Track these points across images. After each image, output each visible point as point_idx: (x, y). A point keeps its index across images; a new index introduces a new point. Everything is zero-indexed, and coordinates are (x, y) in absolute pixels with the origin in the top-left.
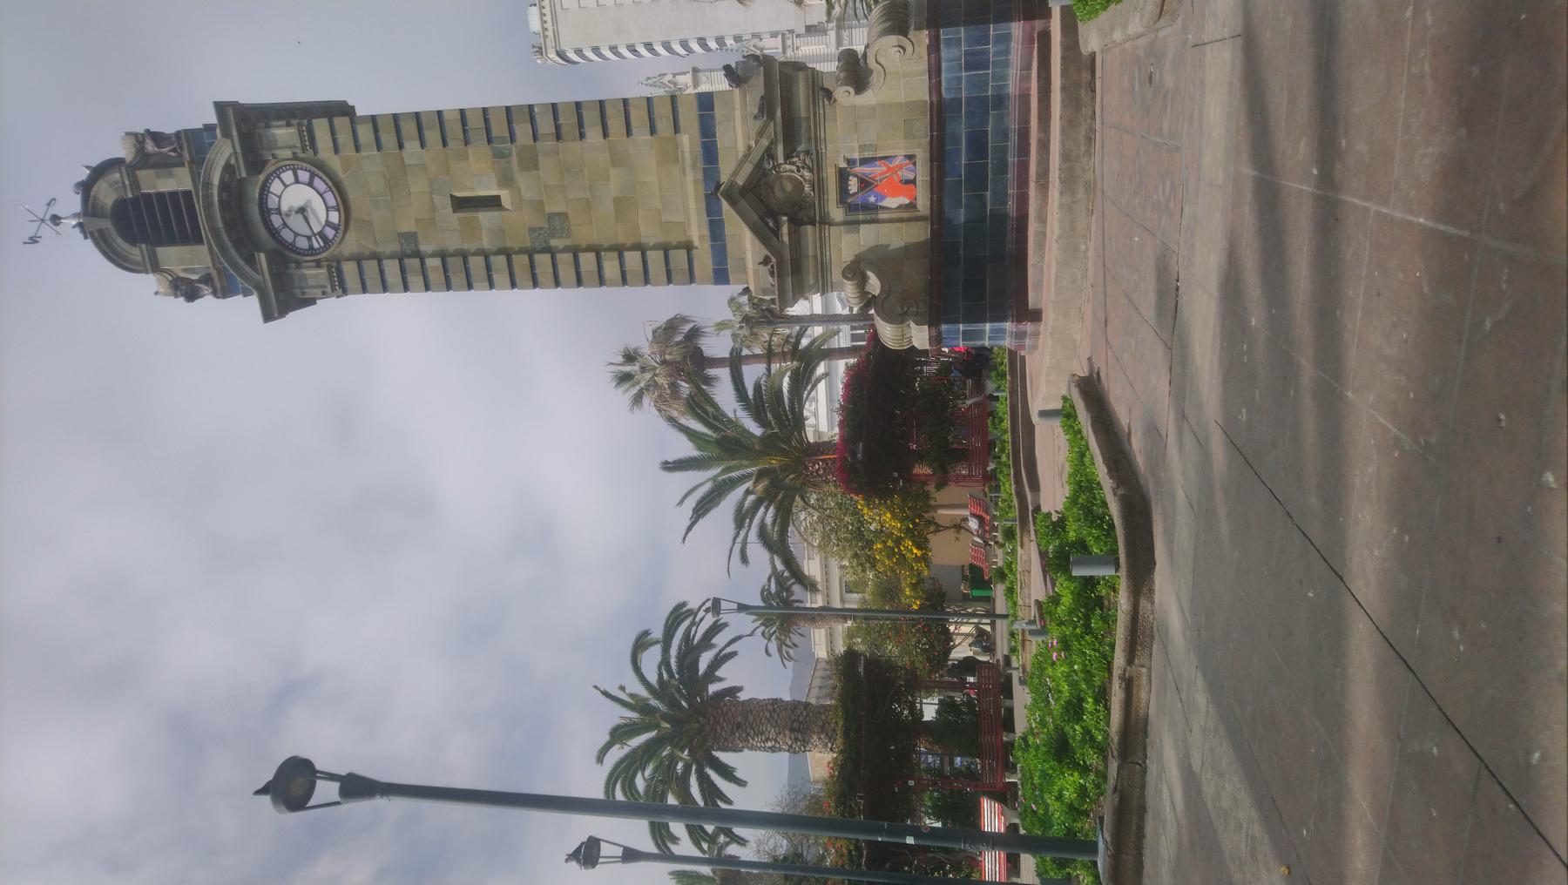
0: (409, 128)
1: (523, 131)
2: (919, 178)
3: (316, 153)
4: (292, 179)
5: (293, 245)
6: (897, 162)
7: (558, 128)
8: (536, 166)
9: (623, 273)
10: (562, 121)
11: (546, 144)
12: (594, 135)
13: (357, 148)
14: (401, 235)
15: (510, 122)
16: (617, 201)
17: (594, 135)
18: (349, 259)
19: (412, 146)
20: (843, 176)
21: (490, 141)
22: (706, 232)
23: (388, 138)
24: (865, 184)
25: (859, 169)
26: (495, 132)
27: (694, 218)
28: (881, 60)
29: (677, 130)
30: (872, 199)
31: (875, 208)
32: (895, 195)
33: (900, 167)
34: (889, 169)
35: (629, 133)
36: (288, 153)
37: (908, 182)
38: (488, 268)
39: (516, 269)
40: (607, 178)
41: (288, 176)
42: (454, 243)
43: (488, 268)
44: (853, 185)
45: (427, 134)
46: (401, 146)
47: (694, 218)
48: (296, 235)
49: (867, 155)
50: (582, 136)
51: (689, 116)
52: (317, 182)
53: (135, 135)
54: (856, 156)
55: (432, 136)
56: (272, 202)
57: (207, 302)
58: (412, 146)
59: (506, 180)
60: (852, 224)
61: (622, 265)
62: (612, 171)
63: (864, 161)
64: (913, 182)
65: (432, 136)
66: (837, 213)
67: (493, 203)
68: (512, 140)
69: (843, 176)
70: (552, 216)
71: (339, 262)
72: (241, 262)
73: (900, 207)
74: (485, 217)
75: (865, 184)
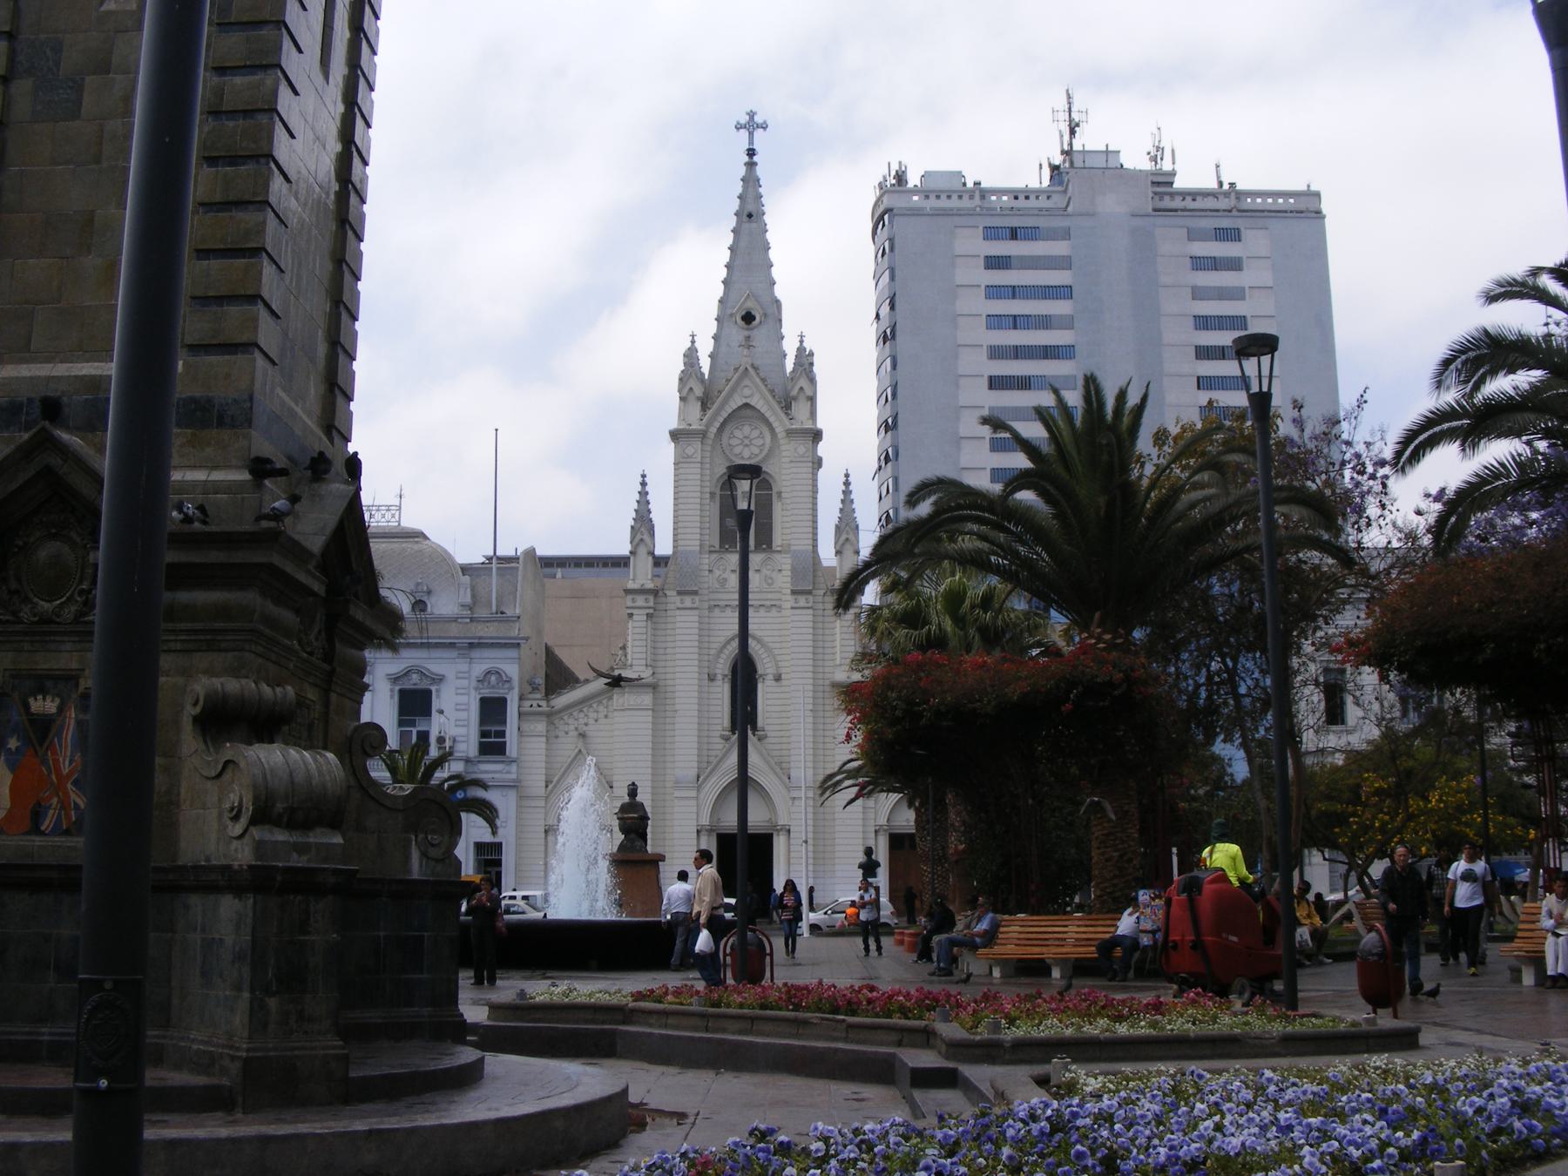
2: (38, 841)
7: (233, 114)
28: (231, 766)
33: (64, 805)
37: (37, 815)
44: (44, 705)
64: (36, 830)
75: (43, 728)
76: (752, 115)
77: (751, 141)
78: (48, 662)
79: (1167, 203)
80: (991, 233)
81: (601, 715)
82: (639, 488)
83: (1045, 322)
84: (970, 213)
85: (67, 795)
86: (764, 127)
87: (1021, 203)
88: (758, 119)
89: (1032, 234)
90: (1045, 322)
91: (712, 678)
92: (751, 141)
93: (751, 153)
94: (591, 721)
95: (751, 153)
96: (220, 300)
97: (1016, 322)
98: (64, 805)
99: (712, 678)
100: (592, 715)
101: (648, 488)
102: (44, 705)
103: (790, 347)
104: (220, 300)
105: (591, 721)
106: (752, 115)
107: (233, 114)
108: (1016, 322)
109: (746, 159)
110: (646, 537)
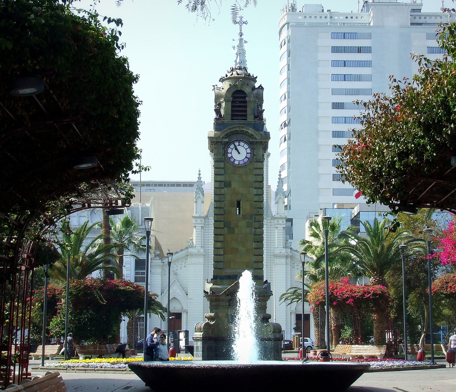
0: (259, 191)
1: (257, 225)
7: (257, 235)
9: (217, 248)
11: (254, 230)
12: (254, 245)
13: (255, 175)
16: (237, 249)
17: (254, 245)
18: (225, 165)
21: (255, 215)
22: (228, 275)
23: (257, 185)
35: (255, 255)
38: (221, 208)
41: (249, 151)
42: (228, 198)
43: (221, 208)
46: (255, 188)
50: (255, 242)
52: (247, 160)
55: (256, 198)
56: (242, 144)
57: (214, 115)
58: (255, 191)
61: (220, 248)
65: (256, 198)
68: (255, 222)
70: (234, 229)
71: (224, 162)
72: (226, 133)
77: (241, 30)
79: (417, 20)
80: (335, 36)
81: (183, 266)
82: (198, 176)
83: (359, 78)
84: (325, 25)
86: (245, 23)
87: (349, 20)
88: (244, 20)
89: (354, 36)
90: (359, 78)
92: (241, 30)
94: (179, 269)
96: (258, 262)
97: (345, 78)
100: (179, 266)
101: (201, 176)
104: (258, 262)
105: (179, 269)
107: (257, 235)
108: (345, 78)
110: (201, 196)
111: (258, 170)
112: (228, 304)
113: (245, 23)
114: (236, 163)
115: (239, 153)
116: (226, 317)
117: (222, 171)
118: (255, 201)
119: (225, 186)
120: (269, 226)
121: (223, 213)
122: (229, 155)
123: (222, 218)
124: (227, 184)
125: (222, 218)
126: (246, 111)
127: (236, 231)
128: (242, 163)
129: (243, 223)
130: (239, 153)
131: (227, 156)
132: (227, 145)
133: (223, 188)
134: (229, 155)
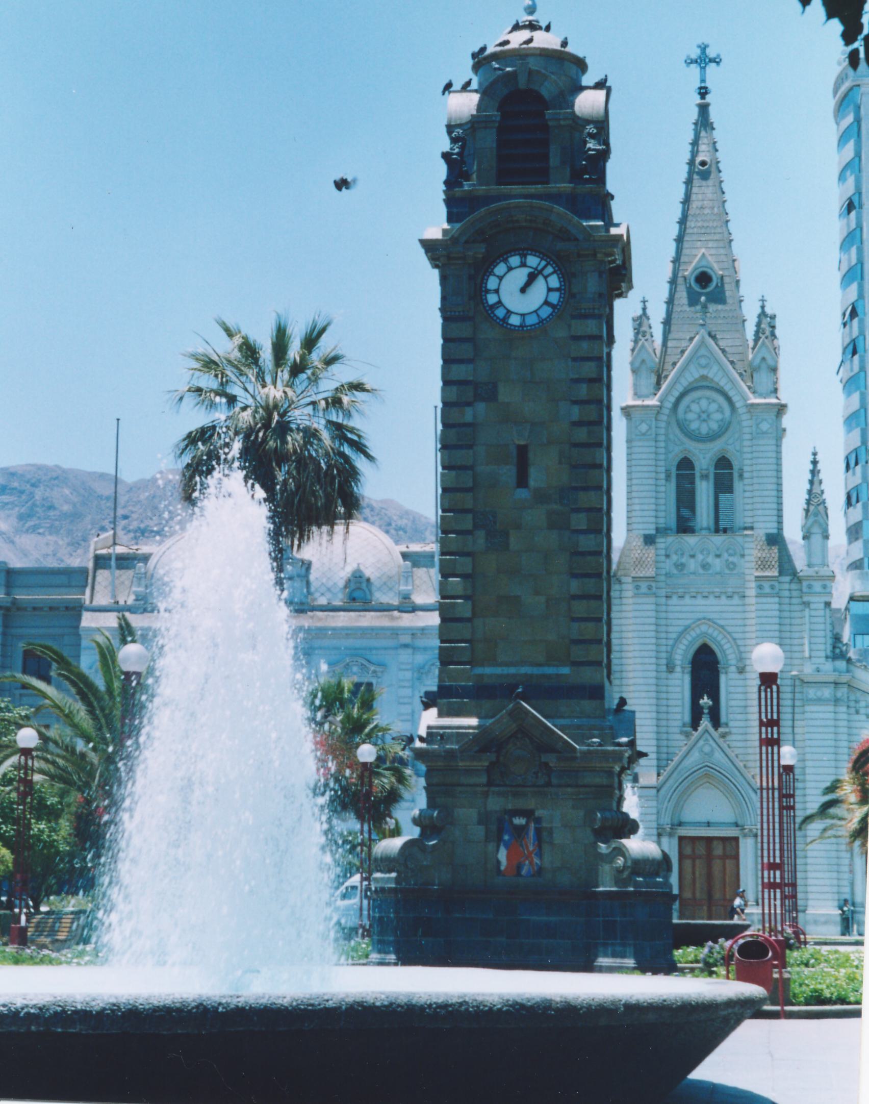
3: (573, 317)
4: (550, 300)
5: (491, 273)
6: (536, 861)
7: (583, 554)
8: (551, 526)
10: (589, 558)
14: (495, 386)
15: (590, 510)
19: (576, 412)
20: (528, 814)
23: (583, 391)
24: (520, 831)
25: (532, 825)
26: (582, 495)
27: (498, 670)
29: (575, 664)
30: (506, 837)
31: (499, 840)
32: (509, 857)
33: (531, 863)
34: (530, 853)
36: (575, 290)
39: (459, 495)
40: (537, 593)
44: (519, 821)
45: (584, 430)
47: (498, 670)
48: (501, 278)
49: (545, 834)
50: (575, 576)
51: (587, 675)
52: (546, 312)
53: (606, 80)
54: (544, 825)
55: (582, 434)
58: (576, 412)
59: (541, 497)
60: (483, 819)
62: (543, 599)
63: (538, 831)
64: (518, 874)
65: (582, 434)
66: (495, 804)
67: (522, 481)
69: (528, 814)
73: (499, 862)
74: (508, 473)
75: (520, 831)
76: (703, 48)
78: (521, 804)
85: (532, 860)
86: (716, 61)
88: (711, 53)
91: (670, 668)
92: (703, 81)
93: (703, 92)
95: (703, 92)
98: (531, 863)
99: (670, 668)
102: (519, 821)
103: (750, 313)
106: (703, 48)
109: (698, 100)
111: (585, 345)
112: (484, 779)
113: (716, 61)
114: (515, 320)
115: (523, 290)
116: (480, 823)
117: (466, 350)
118: (576, 445)
119: (478, 397)
120: (787, 601)
121: (470, 484)
122: (492, 299)
123: (468, 501)
124: (485, 391)
125: (468, 501)
126: (546, 157)
127: (514, 542)
128: (532, 320)
129: (536, 516)
130: (523, 290)
131: (483, 301)
132: (485, 267)
133: (469, 404)
134: (492, 299)
